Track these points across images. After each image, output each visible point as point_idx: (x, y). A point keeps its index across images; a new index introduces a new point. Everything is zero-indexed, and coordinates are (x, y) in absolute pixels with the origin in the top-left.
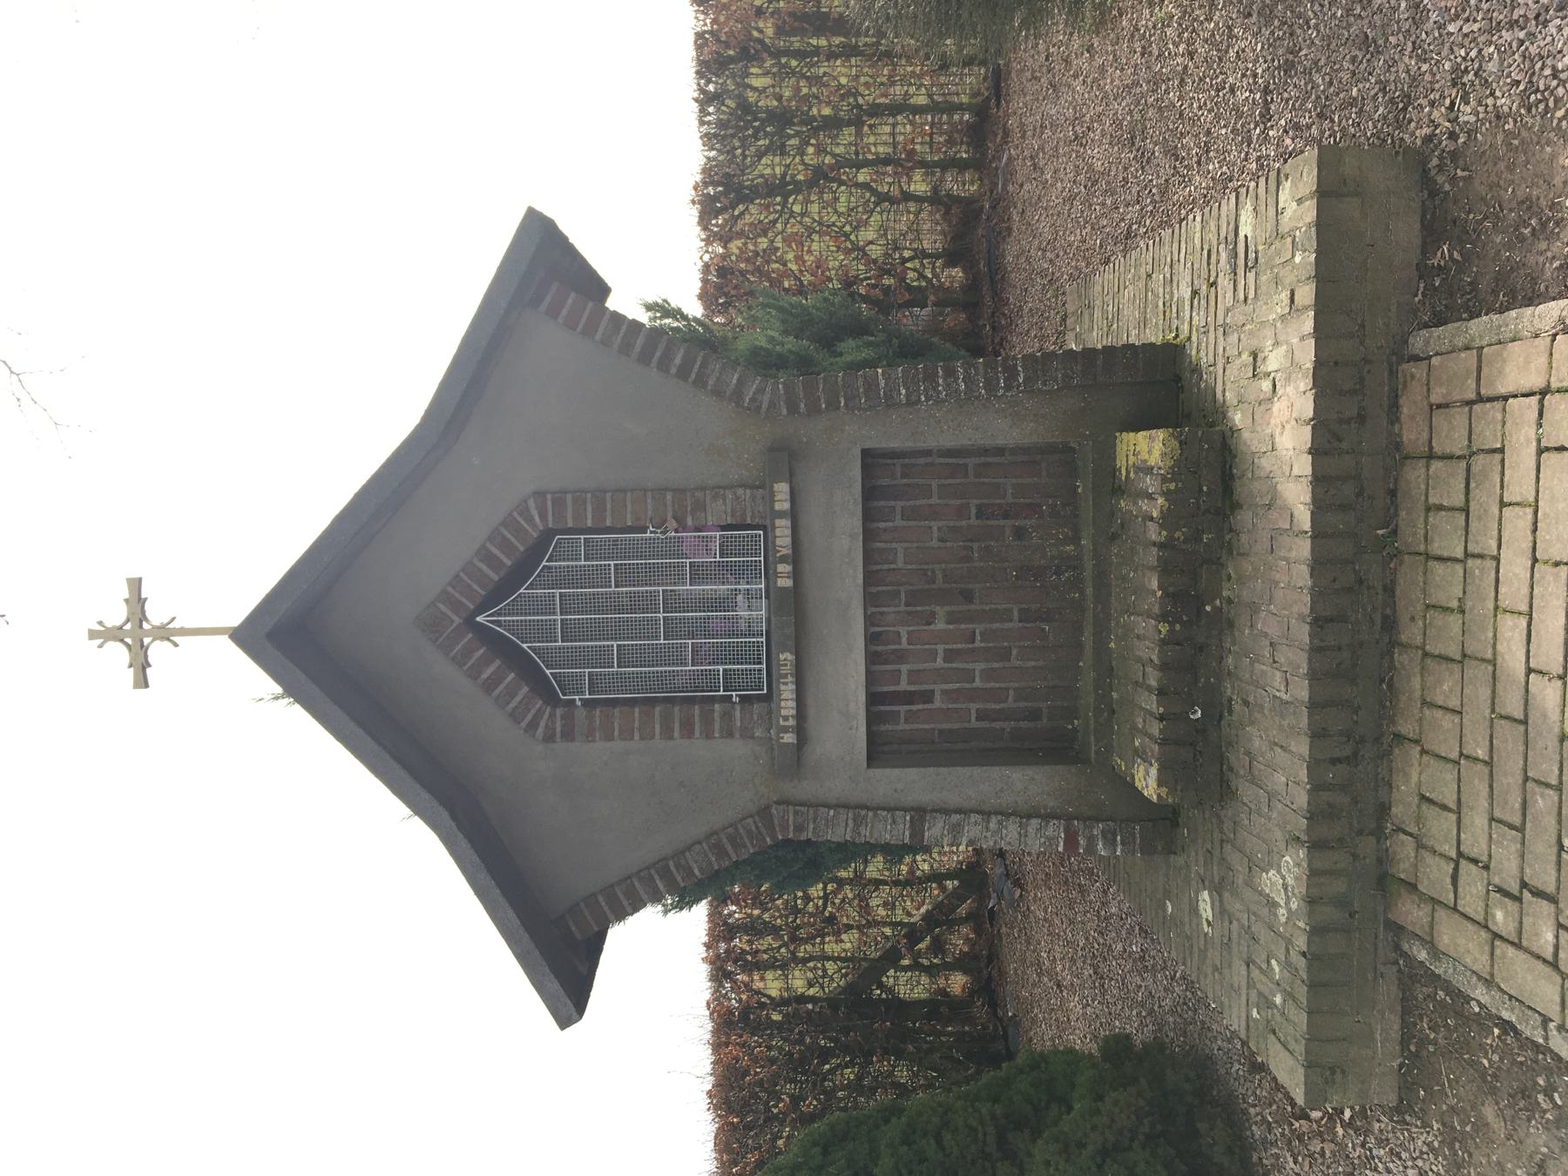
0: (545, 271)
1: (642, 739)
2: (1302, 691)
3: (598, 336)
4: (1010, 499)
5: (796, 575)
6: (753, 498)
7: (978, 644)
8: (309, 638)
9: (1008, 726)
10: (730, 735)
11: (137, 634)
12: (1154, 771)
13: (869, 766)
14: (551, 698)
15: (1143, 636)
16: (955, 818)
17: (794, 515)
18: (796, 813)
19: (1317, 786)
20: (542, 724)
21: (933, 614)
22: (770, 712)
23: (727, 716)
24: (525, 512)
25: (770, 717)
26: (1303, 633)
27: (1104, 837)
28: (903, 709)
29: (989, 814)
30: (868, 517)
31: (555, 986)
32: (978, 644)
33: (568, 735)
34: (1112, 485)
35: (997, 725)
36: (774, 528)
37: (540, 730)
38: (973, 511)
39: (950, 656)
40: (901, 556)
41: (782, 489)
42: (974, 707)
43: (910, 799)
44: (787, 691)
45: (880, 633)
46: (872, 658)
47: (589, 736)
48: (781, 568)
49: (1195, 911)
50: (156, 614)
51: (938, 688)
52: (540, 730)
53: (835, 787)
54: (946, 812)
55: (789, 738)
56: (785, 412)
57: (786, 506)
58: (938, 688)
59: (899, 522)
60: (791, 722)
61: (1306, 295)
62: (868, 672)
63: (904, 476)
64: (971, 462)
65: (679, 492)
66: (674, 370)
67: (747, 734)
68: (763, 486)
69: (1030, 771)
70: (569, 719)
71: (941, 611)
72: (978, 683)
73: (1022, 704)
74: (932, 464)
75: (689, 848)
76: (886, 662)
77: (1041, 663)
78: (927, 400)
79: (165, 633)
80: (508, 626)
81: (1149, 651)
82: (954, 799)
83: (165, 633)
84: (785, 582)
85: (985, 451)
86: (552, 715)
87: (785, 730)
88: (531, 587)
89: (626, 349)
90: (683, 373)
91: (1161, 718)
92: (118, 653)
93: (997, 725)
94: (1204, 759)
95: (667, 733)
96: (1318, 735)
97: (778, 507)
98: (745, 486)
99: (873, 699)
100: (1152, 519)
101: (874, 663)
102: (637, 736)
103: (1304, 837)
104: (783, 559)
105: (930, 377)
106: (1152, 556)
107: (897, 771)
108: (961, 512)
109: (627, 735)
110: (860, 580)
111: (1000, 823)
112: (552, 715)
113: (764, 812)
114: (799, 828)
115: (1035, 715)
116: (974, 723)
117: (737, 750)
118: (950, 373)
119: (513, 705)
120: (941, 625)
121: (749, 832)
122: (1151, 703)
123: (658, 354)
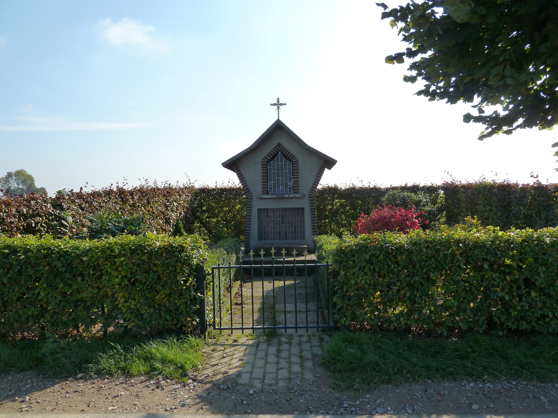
8: (278, 128)
11: (278, 104)
14: (268, 162)
46: (273, 209)
50: (281, 107)
79: (278, 108)
83: (278, 108)
92: (276, 102)
99: (267, 210)
108: (295, 222)
115: (265, 234)
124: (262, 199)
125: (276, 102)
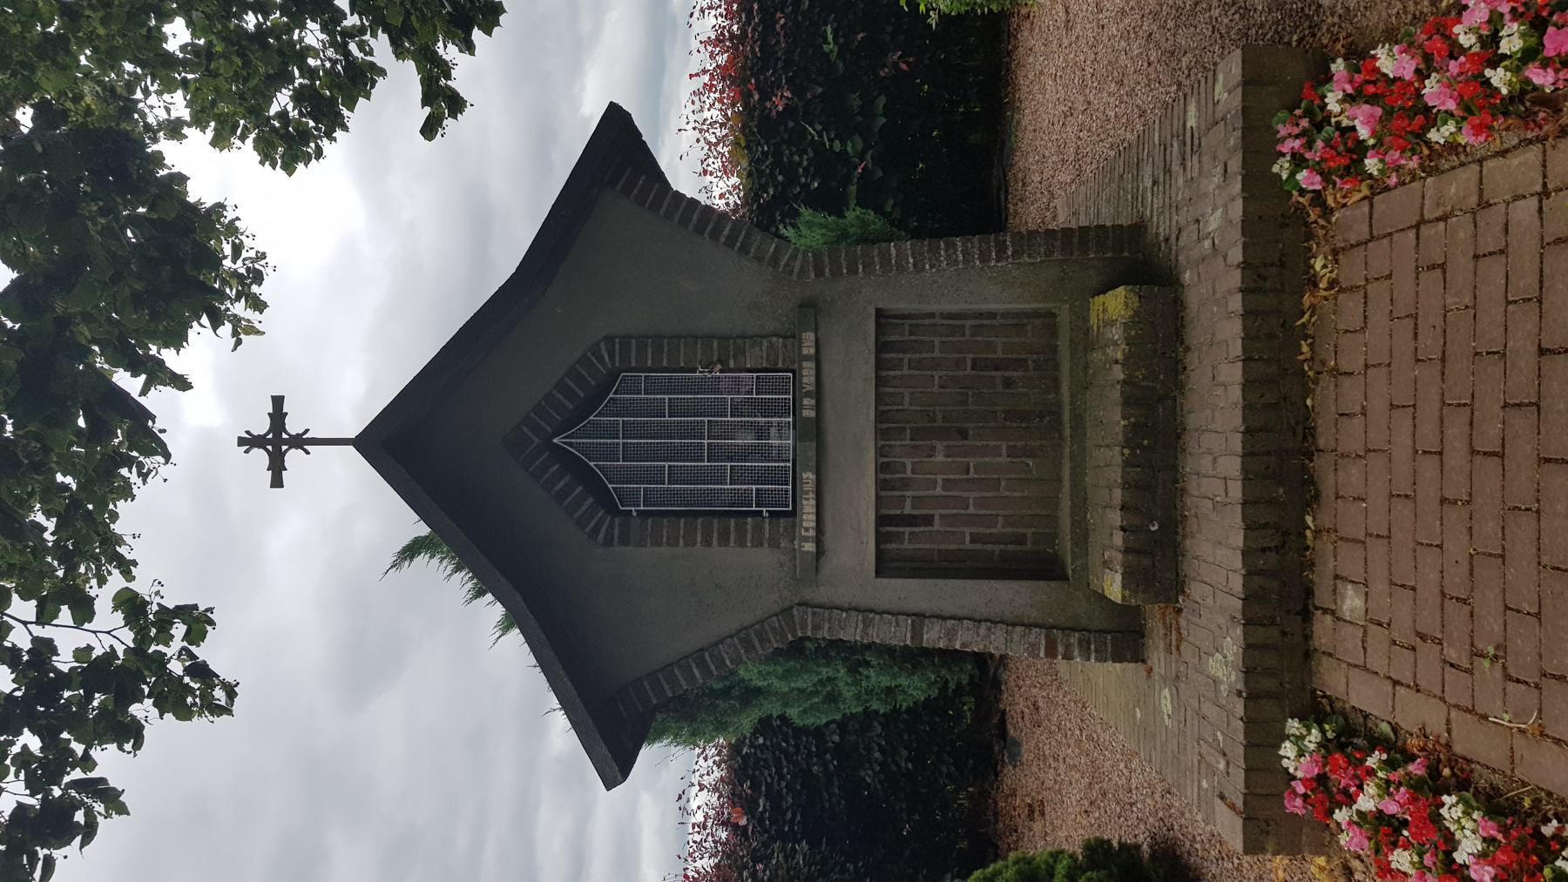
0: (618, 147)
1: (686, 545)
2: (1236, 491)
3: (662, 212)
4: (1000, 354)
5: (818, 407)
6: (785, 346)
7: (972, 475)
9: (997, 548)
10: (761, 544)
12: (1118, 577)
13: (878, 574)
14: (612, 509)
15: (1108, 465)
16: (950, 623)
18: (814, 613)
19: (1250, 574)
20: (603, 530)
21: (933, 448)
22: (794, 526)
23: (758, 529)
25: (792, 532)
26: (1237, 443)
27: (1080, 644)
28: (908, 530)
29: (980, 621)
30: (879, 365)
31: (604, 750)
32: (972, 475)
33: (624, 541)
34: (1086, 340)
35: (989, 547)
36: (801, 368)
37: (601, 535)
38: (969, 364)
40: (907, 399)
41: (809, 337)
42: (968, 531)
43: (912, 606)
44: (808, 506)
45: (888, 464)
46: (881, 485)
47: (641, 543)
48: (806, 401)
49: (1157, 711)
50: (293, 427)
51: (937, 513)
52: (601, 535)
54: (944, 618)
55: (810, 547)
56: (812, 275)
57: (812, 351)
58: (937, 513)
59: (906, 371)
60: (812, 533)
61: (1235, 164)
62: (878, 497)
63: (911, 334)
65: (724, 339)
66: (723, 239)
67: (774, 544)
68: (793, 337)
71: (940, 445)
72: (971, 510)
73: (1010, 530)
74: (935, 325)
75: (722, 641)
76: (893, 489)
77: (1026, 493)
78: (932, 267)
79: (300, 442)
81: (1116, 474)
82: (948, 608)
83: (300, 442)
84: (809, 413)
85: (980, 315)
86: (612, 523)
87: (806, 539)
88: (599, 415)
89: (684, 221)
90: (730, 241)
91: (1123, 529)
92: (260, 457)
93: (989, 547)
94: (1160, 563)
95: (707, 543)
96: (1250, 527)
97: (805, 352)
99: (882, 520)
100: (1117, 362)
101: (883, 489)
102: (681, 542)
103: (1239, 616)
104: (808, 394)
105: (935, 251)
106: (1116, 394)
107: (899, 581)
108: (959, 364)
110: (872, 417)
111: (989, 629)
112: (612, 523)
113: (786, 611)
114: (816, 628)
115: (1020, 540)
116: (968, 545)
117: (762, 559)
119: (579, 513)
121: (773, 629)
122: (1116, 517)
123: (710, 226)
124: (820, 551)
125: (260, 457)
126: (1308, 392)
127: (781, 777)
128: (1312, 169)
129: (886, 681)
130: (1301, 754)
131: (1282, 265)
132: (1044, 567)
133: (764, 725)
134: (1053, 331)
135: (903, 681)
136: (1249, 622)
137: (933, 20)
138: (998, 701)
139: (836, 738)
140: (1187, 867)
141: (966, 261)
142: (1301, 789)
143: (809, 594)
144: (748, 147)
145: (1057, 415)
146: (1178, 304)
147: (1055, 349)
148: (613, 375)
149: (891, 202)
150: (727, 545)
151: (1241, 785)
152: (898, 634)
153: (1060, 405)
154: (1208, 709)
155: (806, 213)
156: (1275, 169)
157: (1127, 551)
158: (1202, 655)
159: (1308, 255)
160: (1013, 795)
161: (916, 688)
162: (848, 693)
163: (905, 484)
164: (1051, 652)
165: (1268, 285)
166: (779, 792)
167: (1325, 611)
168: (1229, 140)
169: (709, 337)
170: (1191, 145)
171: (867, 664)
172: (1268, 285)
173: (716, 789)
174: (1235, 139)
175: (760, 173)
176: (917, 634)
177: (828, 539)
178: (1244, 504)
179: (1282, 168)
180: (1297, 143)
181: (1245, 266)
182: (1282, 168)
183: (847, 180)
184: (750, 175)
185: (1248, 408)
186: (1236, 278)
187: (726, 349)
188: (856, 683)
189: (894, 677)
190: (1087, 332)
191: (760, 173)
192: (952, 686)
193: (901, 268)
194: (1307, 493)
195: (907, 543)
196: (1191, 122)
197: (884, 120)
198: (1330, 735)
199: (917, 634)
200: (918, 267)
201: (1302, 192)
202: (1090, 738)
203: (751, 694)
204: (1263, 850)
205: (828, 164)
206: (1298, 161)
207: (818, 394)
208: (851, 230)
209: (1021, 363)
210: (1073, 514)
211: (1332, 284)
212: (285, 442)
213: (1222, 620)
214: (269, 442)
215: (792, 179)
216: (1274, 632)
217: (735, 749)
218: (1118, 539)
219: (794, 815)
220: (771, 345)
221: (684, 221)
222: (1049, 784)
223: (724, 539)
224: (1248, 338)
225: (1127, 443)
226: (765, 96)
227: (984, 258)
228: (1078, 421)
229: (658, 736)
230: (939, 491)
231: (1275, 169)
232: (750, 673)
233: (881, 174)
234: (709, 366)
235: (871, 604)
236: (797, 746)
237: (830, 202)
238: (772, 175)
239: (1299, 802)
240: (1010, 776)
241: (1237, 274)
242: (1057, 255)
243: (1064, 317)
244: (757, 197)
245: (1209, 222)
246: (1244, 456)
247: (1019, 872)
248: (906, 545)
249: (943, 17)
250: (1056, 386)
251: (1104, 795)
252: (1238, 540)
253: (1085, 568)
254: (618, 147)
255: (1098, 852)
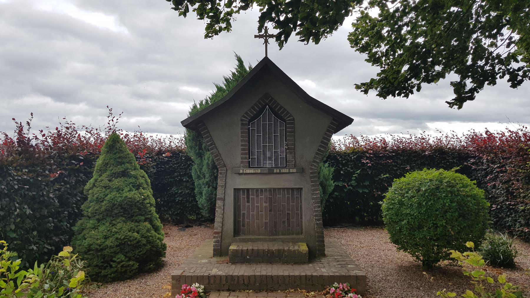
4: (291, 220)
5: (277, 173)
9: (241, 220)
14: (250, 121)
17: (289, 173)
19: (238, 277)
23: (246, 158)
24: (291, 116)
25: (245, 167)
27: (218, 240)
30: (288, 189)
31: (190, 121)
33: (242, 124)
34: (295, 242)
35: (242, 217)
39: (257, 207)
40: (279, 196)
42: (246, 212)
43: (226, 197)
46: (257, 190)
49: (201, 259)
51: (250, 204)
53: (229, 181)
54: (224, 206)
55: (241, 171)
57: (291, 172)
58: (250, 204)
59: (286, 196)
60: (245, 172)
62: (254, 189)
64: (299, 212)
65: (294, 149)
67: (242, 162)
68: (295, 166)
69: (232, 224)
70: (246, 124)
72: (251, 213)
79: (266, 42)
80: (266, 112)
81: (261, 248)
82: (226, 207)
83: (266, 42)
84: (275, 171)
85: (301, 215)
87: (243, 170)
90: (319, 150)
93: (242, 217)
94: (239, 258)
96: (249, 277)
98: (295, 162)
99: (248, 190)
104: (280, 170)
105: (318, 203)
109: (242, 137)
113: (225, 166)
115: (244, 225)
116: (242, 212)
118: (319, 207)
120: (264, 205)
124: (240, 174)
126: (282, 291)
127: (173, 164)
128: (335, 291)
129: (204, 192)
130: (197, 288)
131: (312, 285)
132: (237, 232)
133: (188, 159)
134: (298, 234)
135: (204, 197)
136: (227, 276)
137: (381, 203)
138: (195, 225)
139: (184, 180)
140: (161, 269)
141: (315, 211)
142: (188, 288)
143: (229, 171)
144: (353, 152)
145: (276, 235)
146: (304, 263)
147: (293, 234)
148: (285, 121)
149: (337, 194)
150: (242, 150)
151: (187, 275)
152: (220, 193)
153: (278, 235)
154: (204, 269)
155: (332, 169)
156: (336, 283)
157: (242, 250)
158: (217, 268)
159: (315, 291)
160: (170, 229)
161: (202, 201)
162: (201, 182)
163: (257, 196)
164: (216, 233)
165: (308, 282)
166: (169, 164)
167: (230, 294)
168: (343, 272)
169: (294, 145)
170: (342, 266)
171: (209, 187)
172: (308, 282)
173: (169, 146)
174: (343, 274)
175: (345, 156)
176: (220, 199)
177: (243, 176)
178: (255, 276)
179: (336, 285)
180: (341, 288)
181: (312, 276)
182: (336, 285)
183: (343, 181)
184: (345, 153)
185: (278, 277)
186: (309, 274)
187: (291, 149)
188: (203, 184)
189: (205, 195)
190: (298, 242)
191: (345, 156)
192: (201, 211)
193: (313, 194)
194: (258, 290)
195: (243, 197)
196: (349, 266)
197: (361, 192)
198: (201, 294)
199: (220, 199)
200: (313, 199)
201: (330, 289)
202: (189, 248)
203: (200, 155)
204: (173, 280)
205: (348, 176)
206: (336, 288)
207: (280, 173)
208: (328, 182)
209: (289, 225)
210: (250, 239)
211: (308, 296)
212: (266, 38)
213: (226, 271)
214: (266, 34)
215: (344, 165)
216: (224, 282)
217: (181, 151)
218: (245, 248)
219: (163, 168)
220: (292, 161)
221: (324, 138)
222: (175, 238)
223: (243, 150)
224: (295, 277)
225: (269, 250)
226: (368, 158)
227: (316, 216)
228: (275, 240)
229: (187, 131)
230: (256, 204)
231: (336, 283)
232: (207, 155)
233: (346, 191)
234: (287, 145)
235: (227, 187)
236: (182, 169)
237: (336, 177)
238: (345, 159)
239: (185, 288)
240: (175, 229)
241: (310, 274)
242: (317, 234)
243: (301, 236)
244: (339, 155)
245: (322, 269)
246: (266, 276)
247: (159, 226)
248: (242, 196)
249: (381, 205)
250: (283, 235)
251: (175, 251)
252: (246, 274)
253: (237, 242)
254: (341, 121)
255: (164, 247)
